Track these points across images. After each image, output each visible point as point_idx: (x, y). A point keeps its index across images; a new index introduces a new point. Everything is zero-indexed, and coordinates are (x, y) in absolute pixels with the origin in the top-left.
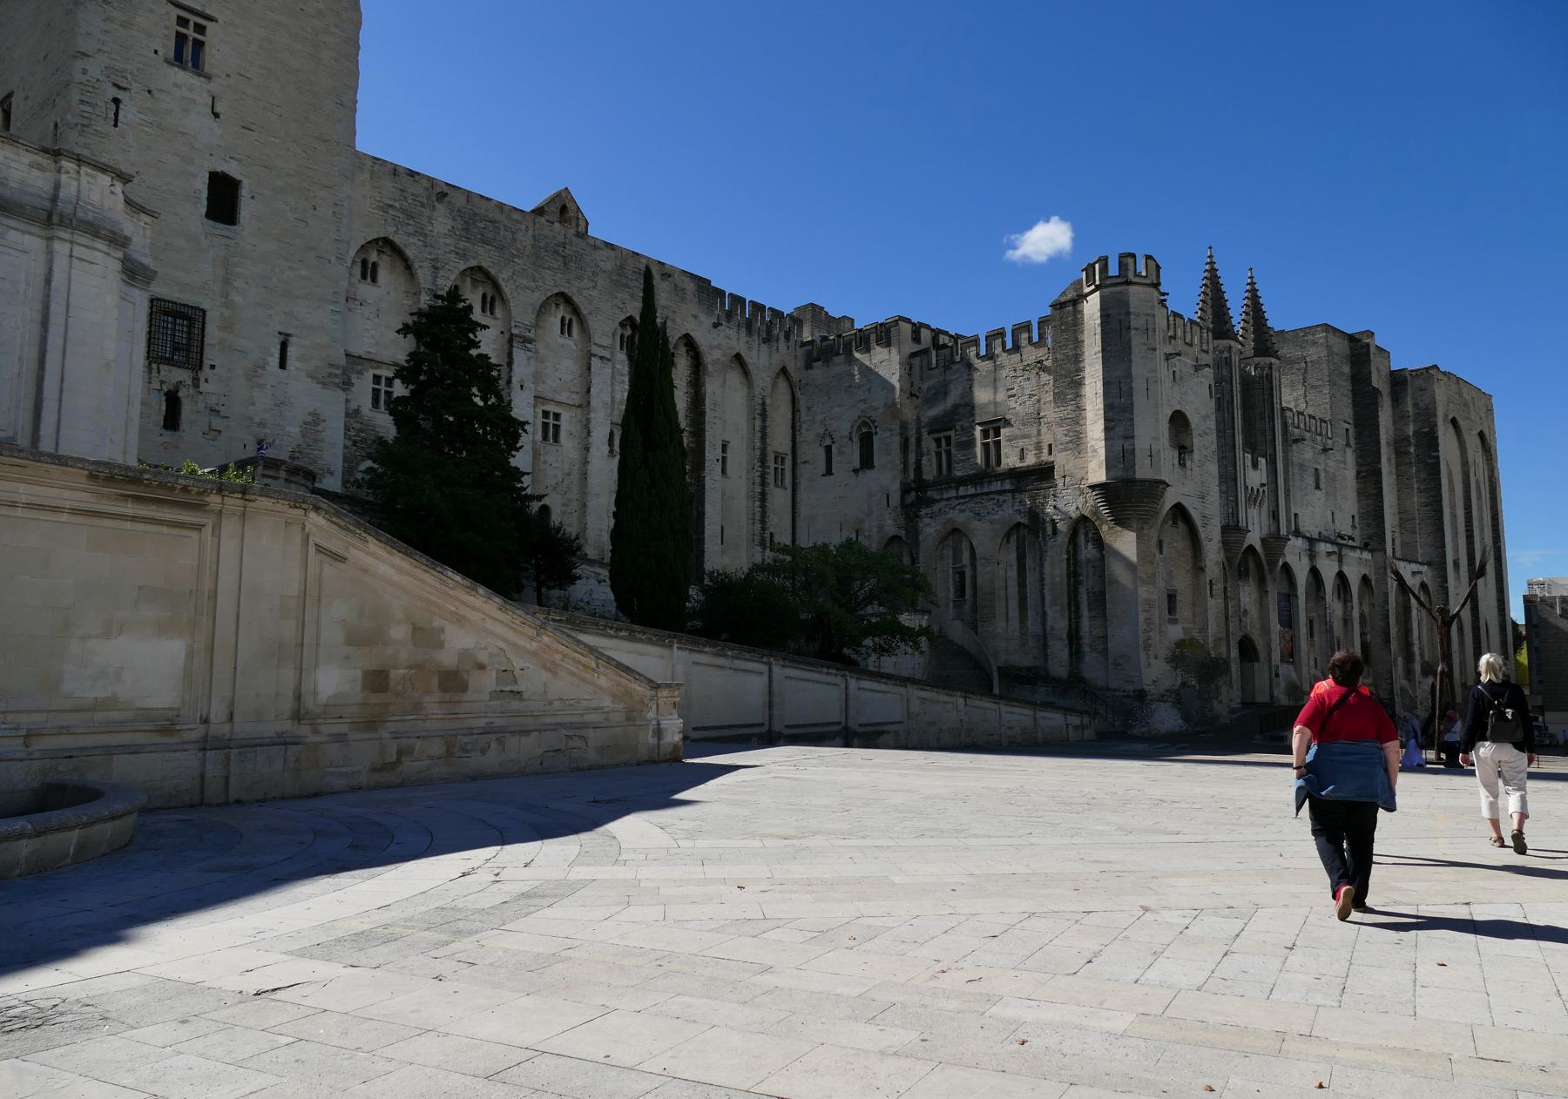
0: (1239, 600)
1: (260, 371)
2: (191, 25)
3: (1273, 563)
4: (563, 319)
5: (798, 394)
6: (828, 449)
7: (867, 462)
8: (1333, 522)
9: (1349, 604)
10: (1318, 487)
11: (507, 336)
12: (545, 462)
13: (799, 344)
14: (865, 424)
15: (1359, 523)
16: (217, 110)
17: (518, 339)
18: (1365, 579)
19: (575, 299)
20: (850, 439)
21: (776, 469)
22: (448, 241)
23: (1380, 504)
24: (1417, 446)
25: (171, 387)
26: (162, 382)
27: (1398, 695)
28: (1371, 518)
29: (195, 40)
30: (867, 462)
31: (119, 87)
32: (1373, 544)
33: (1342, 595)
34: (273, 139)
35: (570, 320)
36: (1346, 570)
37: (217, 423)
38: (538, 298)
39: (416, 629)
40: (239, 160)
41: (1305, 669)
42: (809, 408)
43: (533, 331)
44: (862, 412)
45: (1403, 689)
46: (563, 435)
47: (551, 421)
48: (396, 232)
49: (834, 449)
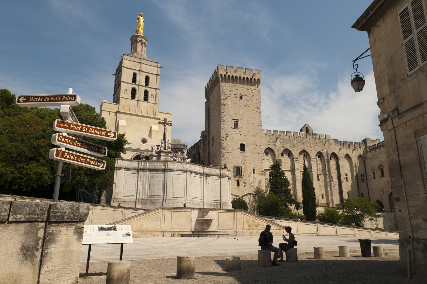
5: (365, 160)
6: (374, 173)
7: (383, 175)
13: (364, 148)
14: (381, 166)
20: (378, 170)
21: (361, 178)
29: (237, 124)
30: (383, 175)
31: (227, 135)
35: (306, 155)
39: (253, 221)
40: (244, 141)
42: (368, 163)
44: (380, 163)
49: (375, 172)
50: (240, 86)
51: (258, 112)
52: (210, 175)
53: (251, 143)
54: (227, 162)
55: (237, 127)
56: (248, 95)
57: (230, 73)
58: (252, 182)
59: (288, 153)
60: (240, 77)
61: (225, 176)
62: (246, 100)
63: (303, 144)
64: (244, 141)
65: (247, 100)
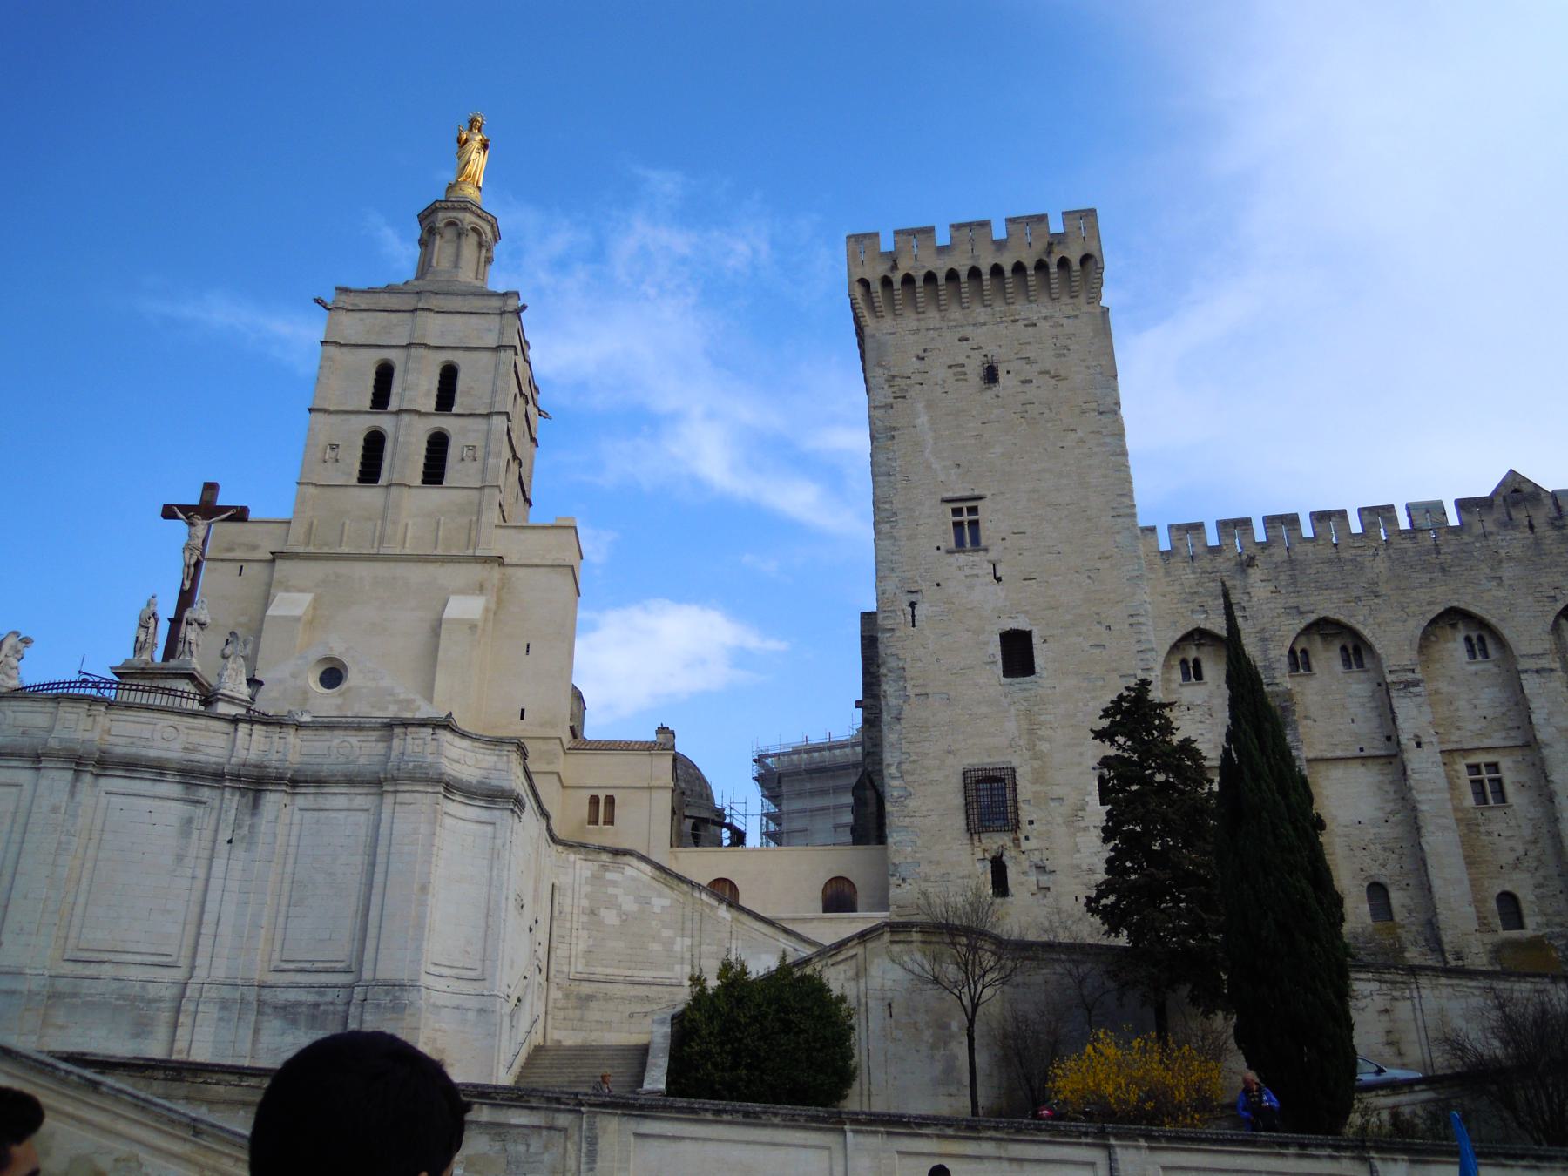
1: (1080, 813)
2: (965, 510)
4: (1468, 639)
11: (1384, 687)
12: (1489, 833)
16: (998, 575)
17: (1396, 687)
19: (1475, 610)
22: (1272, 605)
25: (993, 854)
26: (985, 851)
29: (970, 523)
34: (1055, 578)
35: (1481, 639)
37: (1045, 880)
38: (1416, 627)
40: (1026, 612)
43: (1418, 670)
46: (1509, 789)
47: (1485, 776)
48: (1207, 619)
50: (981, 313)
51: (1105, 431)
52: (294, 782)
53: (1068, 617)
54: (917, 754)
55: (976, 540)
56: (1032, 355)
57: (912, 263)
58: (1096, 860)
59: (1344, 649)
60: (975, 273)
61: (413, 780)
62: (1024, 382)
63: (1443, 570)
64: (1026, 612)
65: (1031, 381)
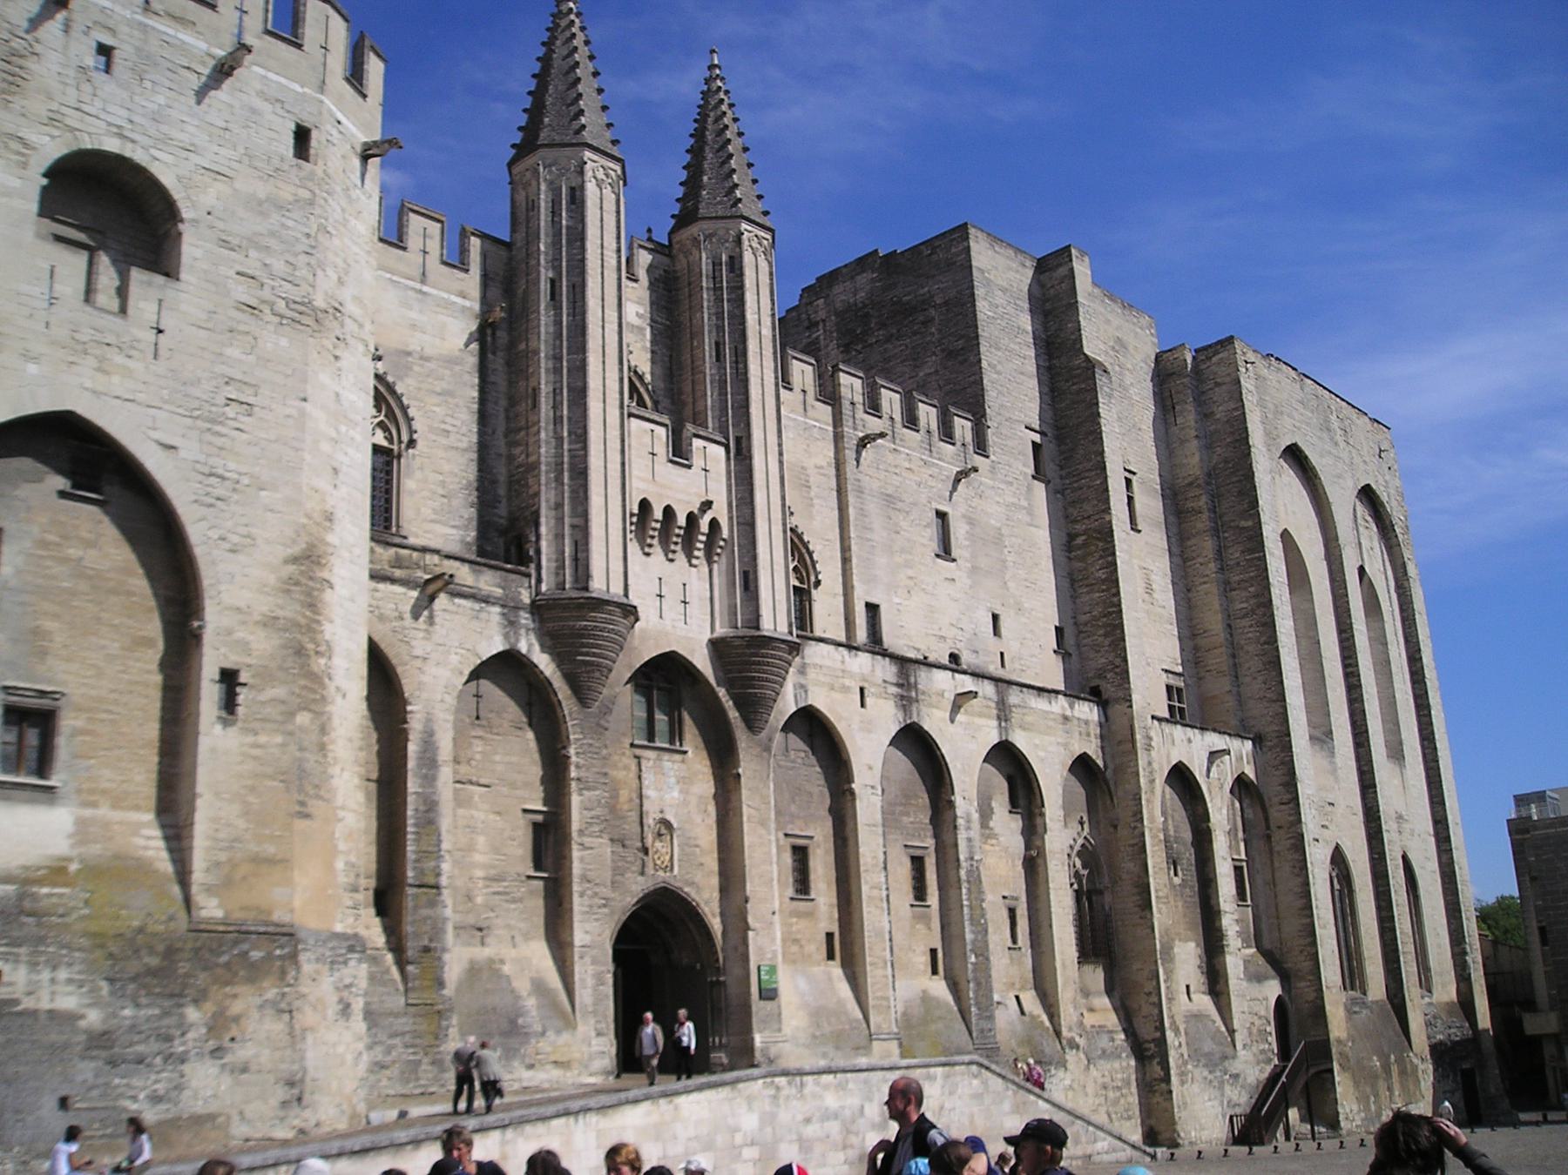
0: (641, 797)
3: (754, 708)
8: (996, 631)
9: (1039, 821)
10: (945, 551)
15: (1078, 646)
18: (1082, 766)
23: (1115, 599)
24: (1215, 497)
27: (1177, 1031)
28: (1101, 632)
32: (1109, 690)
33: (1022, 802)
36: (1020, 740)
41: (875, 975)
45: (1197, 1017)
